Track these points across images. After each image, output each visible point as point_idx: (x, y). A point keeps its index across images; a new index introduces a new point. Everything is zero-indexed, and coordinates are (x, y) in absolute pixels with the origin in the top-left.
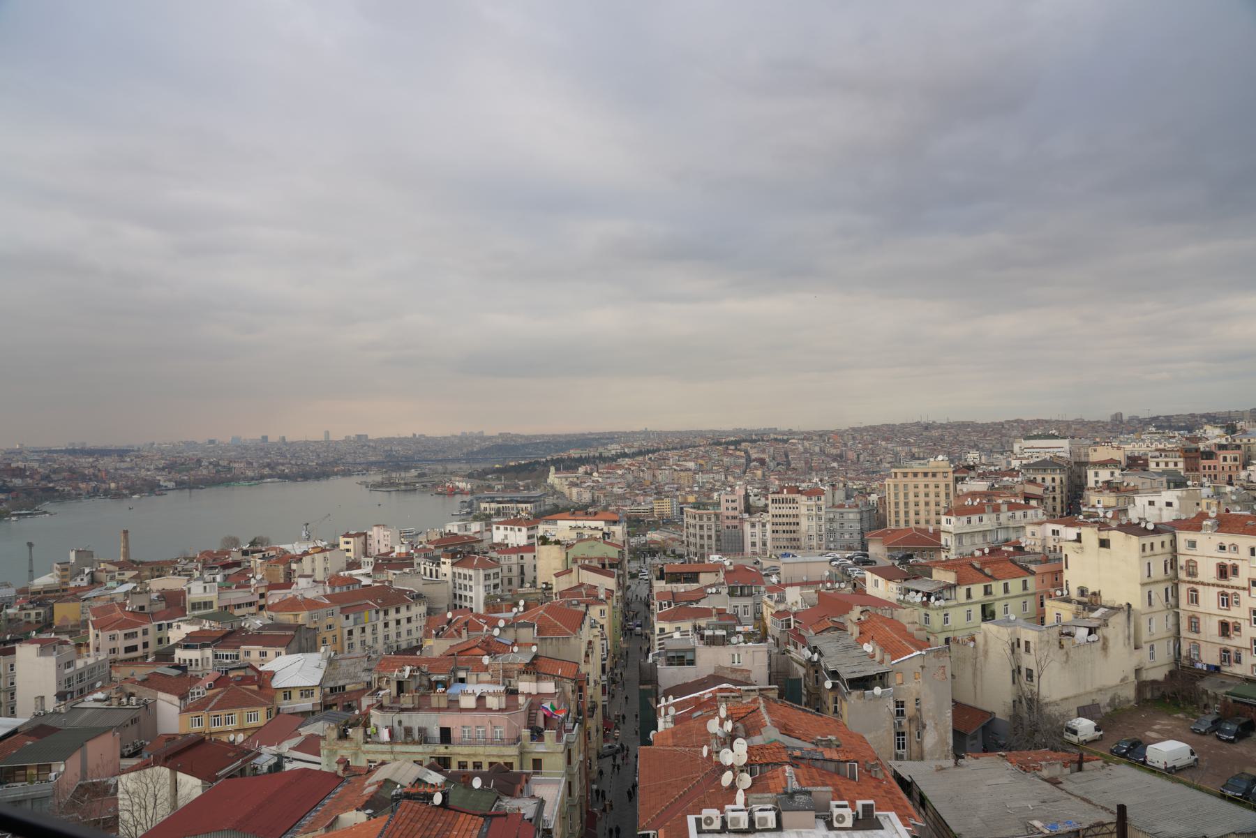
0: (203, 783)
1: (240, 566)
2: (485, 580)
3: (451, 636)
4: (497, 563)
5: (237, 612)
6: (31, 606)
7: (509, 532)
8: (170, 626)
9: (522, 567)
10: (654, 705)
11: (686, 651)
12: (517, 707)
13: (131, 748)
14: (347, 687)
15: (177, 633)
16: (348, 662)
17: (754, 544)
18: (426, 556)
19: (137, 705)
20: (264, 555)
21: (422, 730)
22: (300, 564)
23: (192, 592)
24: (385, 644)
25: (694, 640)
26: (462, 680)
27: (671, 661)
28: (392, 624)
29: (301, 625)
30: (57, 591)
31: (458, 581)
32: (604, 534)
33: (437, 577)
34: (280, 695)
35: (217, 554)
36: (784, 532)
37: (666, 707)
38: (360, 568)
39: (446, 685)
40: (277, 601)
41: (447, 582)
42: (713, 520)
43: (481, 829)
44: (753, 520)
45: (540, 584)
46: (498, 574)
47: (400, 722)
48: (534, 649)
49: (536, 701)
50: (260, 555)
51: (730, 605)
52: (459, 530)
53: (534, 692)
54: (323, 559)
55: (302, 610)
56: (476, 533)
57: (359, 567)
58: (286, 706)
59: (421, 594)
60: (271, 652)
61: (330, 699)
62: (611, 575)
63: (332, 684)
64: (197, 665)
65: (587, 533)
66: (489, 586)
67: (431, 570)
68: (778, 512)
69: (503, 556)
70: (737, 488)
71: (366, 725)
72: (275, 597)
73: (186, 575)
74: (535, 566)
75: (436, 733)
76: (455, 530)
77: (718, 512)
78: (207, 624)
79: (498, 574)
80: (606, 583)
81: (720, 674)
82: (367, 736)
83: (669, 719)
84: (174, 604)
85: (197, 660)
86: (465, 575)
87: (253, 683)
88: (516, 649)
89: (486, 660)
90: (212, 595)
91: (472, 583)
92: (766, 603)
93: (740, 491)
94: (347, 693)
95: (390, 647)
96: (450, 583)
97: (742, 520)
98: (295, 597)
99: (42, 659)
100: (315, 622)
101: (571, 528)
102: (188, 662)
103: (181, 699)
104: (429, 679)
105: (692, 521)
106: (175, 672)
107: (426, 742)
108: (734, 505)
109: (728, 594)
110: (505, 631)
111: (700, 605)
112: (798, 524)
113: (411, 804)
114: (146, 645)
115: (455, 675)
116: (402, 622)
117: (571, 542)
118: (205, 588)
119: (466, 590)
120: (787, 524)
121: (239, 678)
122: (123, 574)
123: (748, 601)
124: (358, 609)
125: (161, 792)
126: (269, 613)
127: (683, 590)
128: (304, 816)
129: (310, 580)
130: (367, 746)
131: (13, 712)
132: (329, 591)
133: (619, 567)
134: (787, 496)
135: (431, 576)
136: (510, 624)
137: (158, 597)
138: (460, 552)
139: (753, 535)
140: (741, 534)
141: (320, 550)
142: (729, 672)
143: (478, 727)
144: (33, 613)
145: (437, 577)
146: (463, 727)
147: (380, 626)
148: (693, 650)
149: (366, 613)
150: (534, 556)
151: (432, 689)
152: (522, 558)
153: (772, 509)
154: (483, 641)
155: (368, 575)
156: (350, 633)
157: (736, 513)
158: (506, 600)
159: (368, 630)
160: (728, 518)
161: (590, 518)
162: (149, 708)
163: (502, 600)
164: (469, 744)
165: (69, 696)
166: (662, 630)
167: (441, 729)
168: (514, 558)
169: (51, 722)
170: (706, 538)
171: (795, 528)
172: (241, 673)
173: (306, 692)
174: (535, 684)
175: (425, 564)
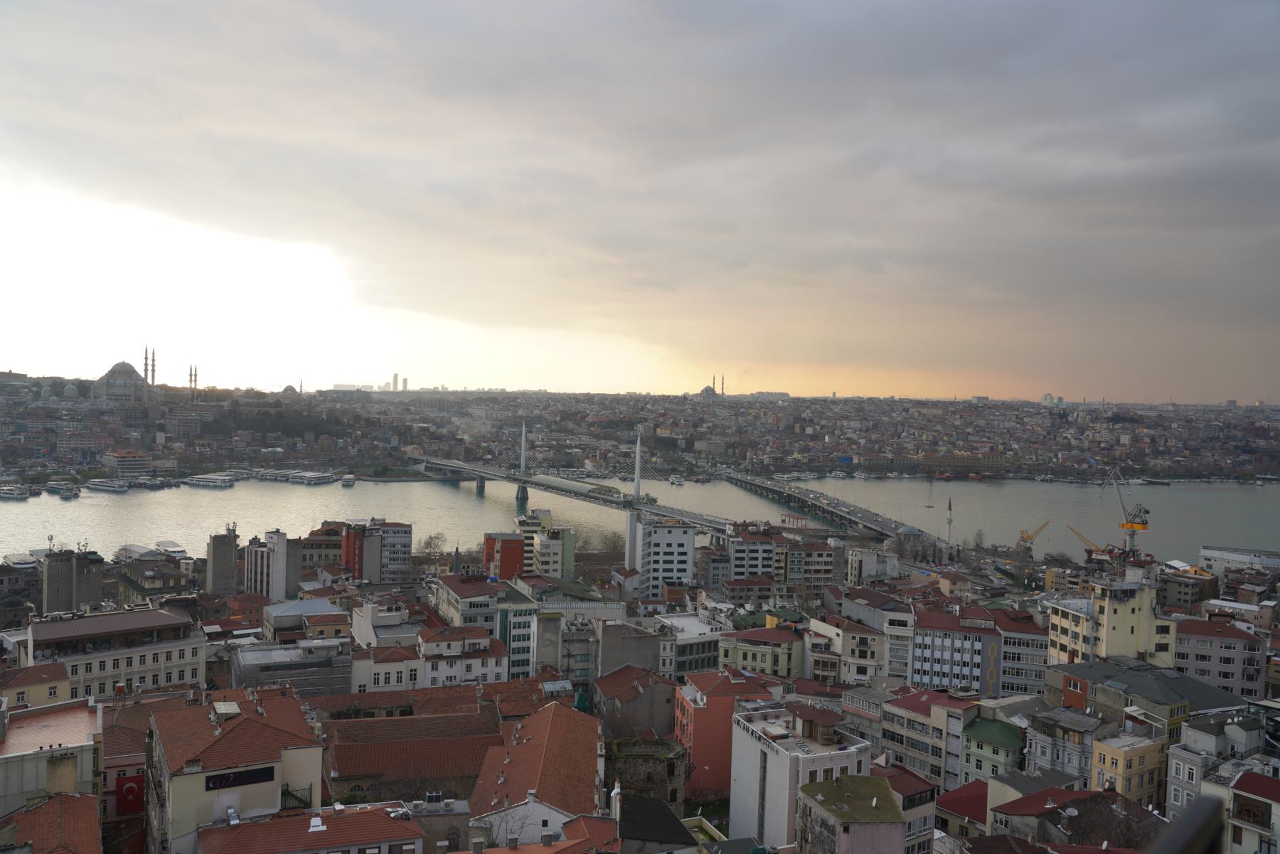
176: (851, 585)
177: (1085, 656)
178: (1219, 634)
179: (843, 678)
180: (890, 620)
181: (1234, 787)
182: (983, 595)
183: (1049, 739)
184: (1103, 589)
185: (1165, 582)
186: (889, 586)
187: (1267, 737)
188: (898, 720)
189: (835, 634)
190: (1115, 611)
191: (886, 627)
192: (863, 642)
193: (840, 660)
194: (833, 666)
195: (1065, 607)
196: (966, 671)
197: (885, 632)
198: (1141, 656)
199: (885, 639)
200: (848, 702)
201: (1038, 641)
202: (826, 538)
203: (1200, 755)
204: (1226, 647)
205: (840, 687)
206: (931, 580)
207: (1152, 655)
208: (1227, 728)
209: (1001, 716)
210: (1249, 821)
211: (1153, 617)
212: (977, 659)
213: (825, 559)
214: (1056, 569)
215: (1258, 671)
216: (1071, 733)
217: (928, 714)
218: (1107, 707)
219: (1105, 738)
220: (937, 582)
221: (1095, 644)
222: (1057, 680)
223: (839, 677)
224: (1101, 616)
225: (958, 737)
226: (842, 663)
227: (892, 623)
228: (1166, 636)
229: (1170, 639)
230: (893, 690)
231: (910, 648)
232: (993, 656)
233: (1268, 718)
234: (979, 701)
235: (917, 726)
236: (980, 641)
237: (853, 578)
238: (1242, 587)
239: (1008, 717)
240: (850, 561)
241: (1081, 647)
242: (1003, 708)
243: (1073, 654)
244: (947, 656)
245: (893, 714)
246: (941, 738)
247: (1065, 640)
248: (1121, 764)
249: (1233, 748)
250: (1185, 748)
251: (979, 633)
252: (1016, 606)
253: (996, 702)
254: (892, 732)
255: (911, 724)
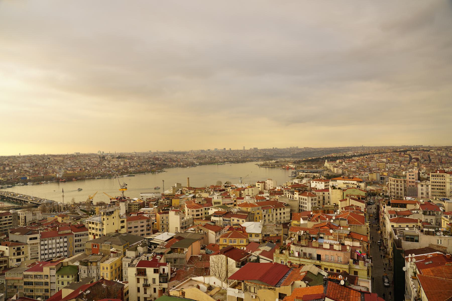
0: (236, 262)
1: (225, 191)
2: (311, 201)
3: (314, 221)
4: (315, 195)
5: (229, 206)
6: (166, 199)
7: (317, 184)
8: (209, 209)
9: (324, 197)
10: (403, 257)
11: (415, 236)
12: (346, 250)
13: (202, 247)
14: (270, 235)
15: (211, 211)
16: (269, 226)
17: (422, 194)
18: (288, 191)
19: (203, 233)
20: (232, 188)
21: (310, 254)
22: (244, 191)
23: (214, 198)
24: (276, 221)
25: (417, 232)
26: (321, 238)
27: (407, 239)
28: (278, 214)
29: (250, 212)
30: (172, 195)
31: (301, 201)
32: (357, 186)
33: (293, 199)
34: (249, 236)
35: (216, 186)
36: (437, 189)
37: (411, 258)
38: (263, 194)
39: (316, 239)
40: (240, 203)
41: (297, 201)
42: (403, 182)
43: (361, 297)
44: (422, 183)
45: (332, 203)
46: (316, 199)
47: (302, 250)
48: (349, 229)
49: (353, 249)
50: (230, 188)
51: (424, 218)
52: (298, 182)
53: (352, 246)
54: (251, 190)
55: (249, 207)
56: (304, 183)
57: (263, 194)
58: (251, 239)
59: (288, 205)
60: (241, 220)
61: (265, 238)
62: (363, 202)
63: (265, 233)
64: (218, 222)
65: (351, 186)
66: (313, 203)
67: (291, 196)
68: (434, 181)
69: (316, 192)
70: (414, 170)
71: (289, 250)
72: (239, 202)
73: (208, 193)
74: (329, 197)
75: (315, 256)
76: (297, 182)
77: (405, 179)
78: (220, 209)
79: (316, 199)
80: (362, 206)
81: (431, 247)
82: (290, 254)
83: (412, 263)
84: (209, 202)
85: (218, 221)
86: (304, 199)
87: (241, 230)
88: (342, 228)
89: (331, 231)
90: (220, 200)
91: (306, 202)
92: (444, 219)
93: (415, 171)
94: (270, 237)
95: (278, 222)
96: (298, 201)
97: (417, 183)
98: (247, 202)
99: (176, 216)
100: (254, 211)
101: (344, 183)
102: (215, 221)
103: (215, 233)
104: (310, 236)
105: (393, 183)
106: (213, 224)
107: (312, 259)
108: (413, 177)
109: (423, 214)
110: (335, 221)
111: (409, 217)
112: (445, 186)
113: (332, 283)
114: (202, 214)
115: (319, 236)
116: (282, 214)
117: (345, 189)
118: (218, 197)
119: (304, 204)
120: (439, 186)
121: (237, 228)
122: (190, 191)
123: (433, 218)
124: (268, 208)
125: (223, 263)
126: (239, 207)
127: (399, 211)
128: (281, 280)
129: (249, 197)
130: (290, 257)
131: (167, 231)
132: (256, 201)
133: (365, 199)
134: (439, 174)
135: (291, 198)
136: (337, 218)
137: (204, 199)
138: (302, 190)
139: (422, 190)
140: (416, 189)
141: (250, 187)
142: (436, 246)
143: (331, 256)
144: (166, 201)
145: (293, 199)
146: (326, 255)
147: (275, 214)
148: (418, 236)
149: (270, 210)
150: (329, 193)
151: (311, 240)
152: (324, 193)
153: (432, 179)
154: (327, 224)
155: (268, 197)
156: (265, 216)
157: (414, 180)
158: (321, 209)
159: (271, 216)
160: (410, 182)
161: (350, 180)
162: (206, 234)
163: (319, 209)
164: (328, 262)
165: (184, 228)
166: (392, 226)
167: (317, 255)
168: (321, 193)
169: (181, 235)
170: (399, 190)
171: (443, 188)
172: (237, 226)
173: (257, 235)
174: (352, 242)
175: (288, 194)
176: (22, 226)
177: (100, 235)
178: (140, 219)
179: (10, 265)
180: (30, 238)
181: (137, 267)
182: (73, 220)
183: (86, 267)
184: (104, 213)
185: (131, 205)
186: (38, 223)
187: (148, 247)
188: (30, 277)
189: (6, 249)
190: (108, 219)
191: (28, 241)
192: (19, 249)
193: (8, 259)
194: (5, 261)
195: (93, 221)
196: (62, 250)
197: (28, 243)
198: (117, 231)
199: (28, 246)
200: (8, 275)
201: (86, 233)
202: (9, 210)
203: (131, 258)
204: (142, 223)
205: (7, 268)
206: (54, 218)
207: (120, 230)
208: (138, 248)
209: (70, 264)
210: (141, 275)
211: (119, 218)
212: (66, 244)
213: (8, 218)
214: (99, 207)
215: (150, 227)
216: (93, 263)
217: (42, 271)
218: (105, 250)
219: (104, 261)
220: (57, 219)
221: (103, 231)
222: (89, 246)
223: (8, 265)
224: (104, 221)
225: (55, 276)
226: (10, 260)
227: (31, 239)
228: (124, 223)
229: (125, 224)
230: (28, 265)
231: (39, 247)
232: (71, 242)
233: (148, 242)
234: (62, 260)
235: (38, 276)
236: (66, 238)
237: (23, 224)
238: (150, 203)
239: (72, 263)
240: (21, 217)
241: (98, 233)
242: (71, 261)
243: (97, 235)
244: (54, 246)
245: (28, 275)
246: (48, 278)
247: (94, 231)
248: (109, 268)
249: (140, 253)
250: (127, 258)
251: (65, 235)
252: (79, 223)
253: (69, 259)
254: (28, 282)
255: (36, 276)
